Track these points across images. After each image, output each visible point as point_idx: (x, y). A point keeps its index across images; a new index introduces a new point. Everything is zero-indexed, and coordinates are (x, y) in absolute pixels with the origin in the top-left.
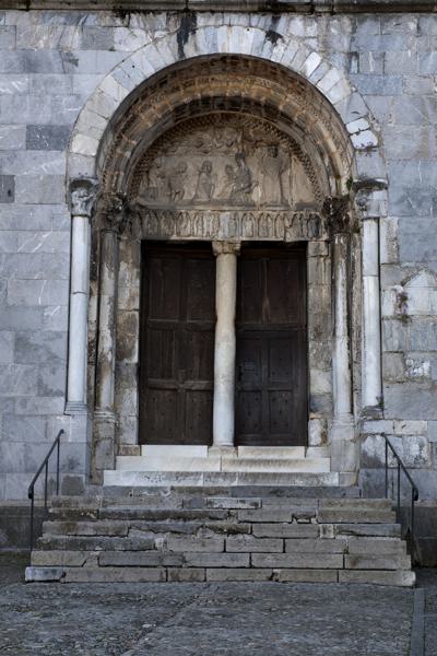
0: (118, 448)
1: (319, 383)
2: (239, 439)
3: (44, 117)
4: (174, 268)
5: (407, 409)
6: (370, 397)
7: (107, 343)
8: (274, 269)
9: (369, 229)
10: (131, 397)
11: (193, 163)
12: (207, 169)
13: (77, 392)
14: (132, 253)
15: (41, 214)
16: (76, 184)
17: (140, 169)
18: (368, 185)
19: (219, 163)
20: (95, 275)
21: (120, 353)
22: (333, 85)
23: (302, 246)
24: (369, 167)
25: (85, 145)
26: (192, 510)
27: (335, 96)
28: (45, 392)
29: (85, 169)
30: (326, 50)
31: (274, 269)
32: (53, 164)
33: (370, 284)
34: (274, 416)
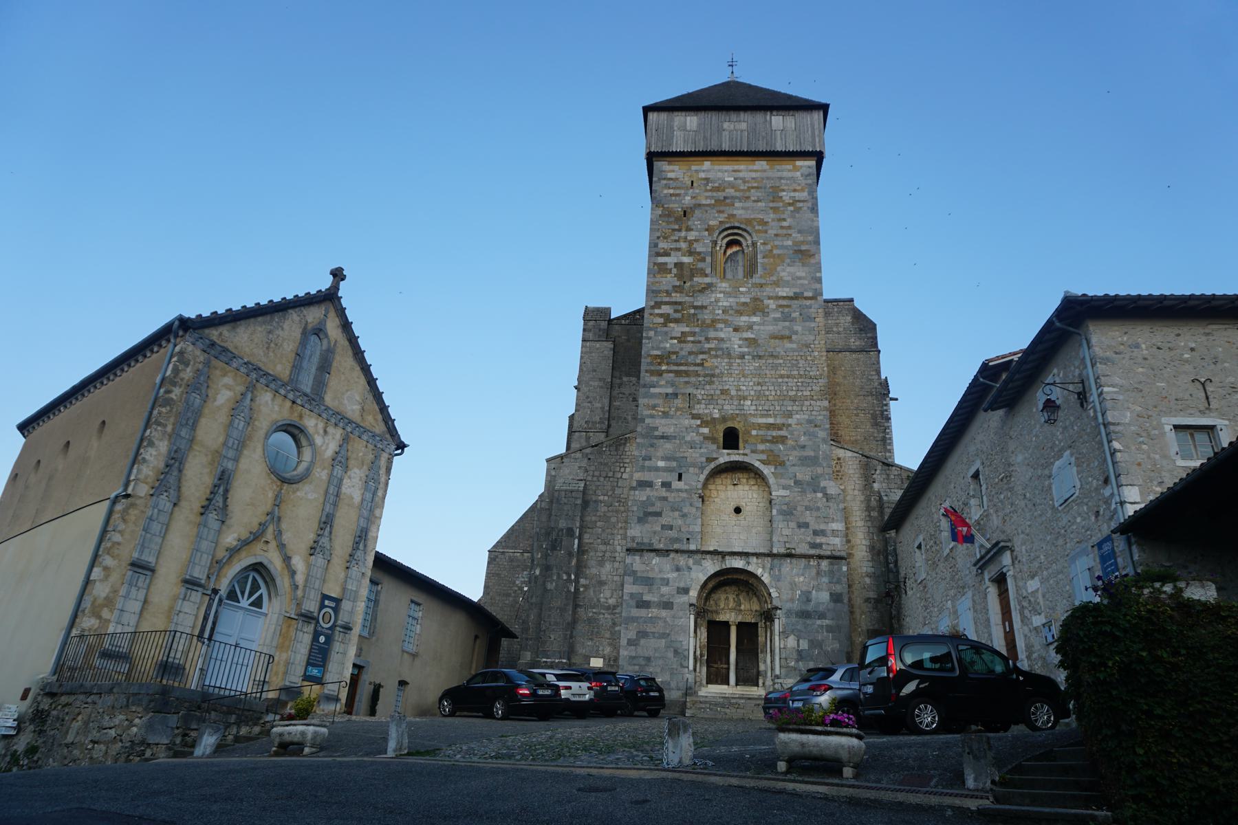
0: (701, 685)
1: (762, 667)
2: (737, 685)
3: (682, 585)
4: (717, 631)
5: (787, 676)
6: (777, 672)
7: (698, 653)
8: (748, 631)
9: (777, 621)
10: (704, 669)
11: (723, 597)
12: (727, 599)
13: (691, 667)
14: (705, 624)
15: (681, 613)
16: (691, 605)
17: (707, 598)
18: (777, 608)
19: (731, 597)
20: (695, 632)
21: (702, 655)
22: (766, 579)
23: (756, 624)
24: (776, 603)
25: (694, 593)
26: (727, 701)
27: (766, 581)
28: (682, 666)
29: (694, 601)
30: (764, 568)
31: (748, 631)
32: (684, 599)
33: (777, 638)
34: (749, 677)
